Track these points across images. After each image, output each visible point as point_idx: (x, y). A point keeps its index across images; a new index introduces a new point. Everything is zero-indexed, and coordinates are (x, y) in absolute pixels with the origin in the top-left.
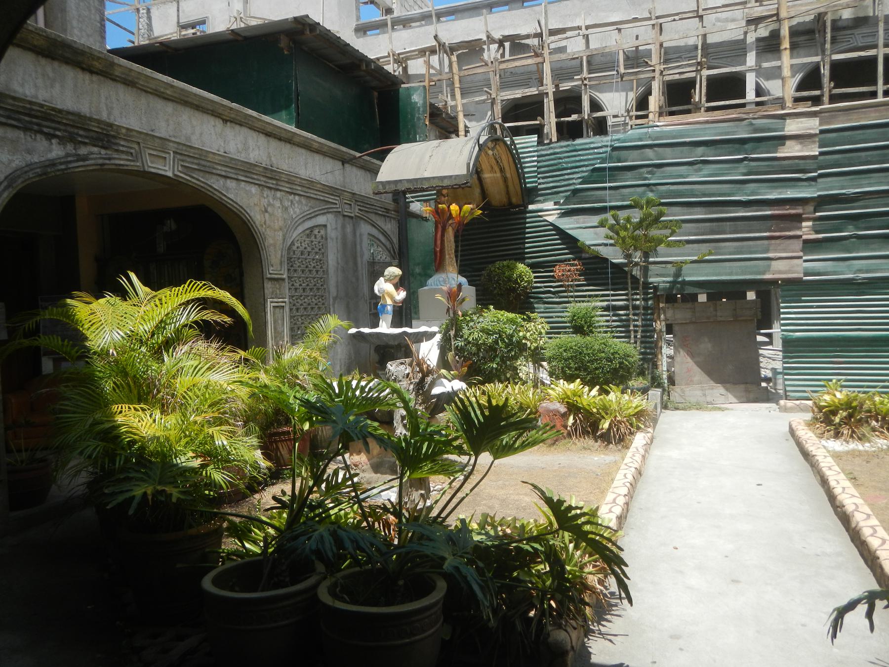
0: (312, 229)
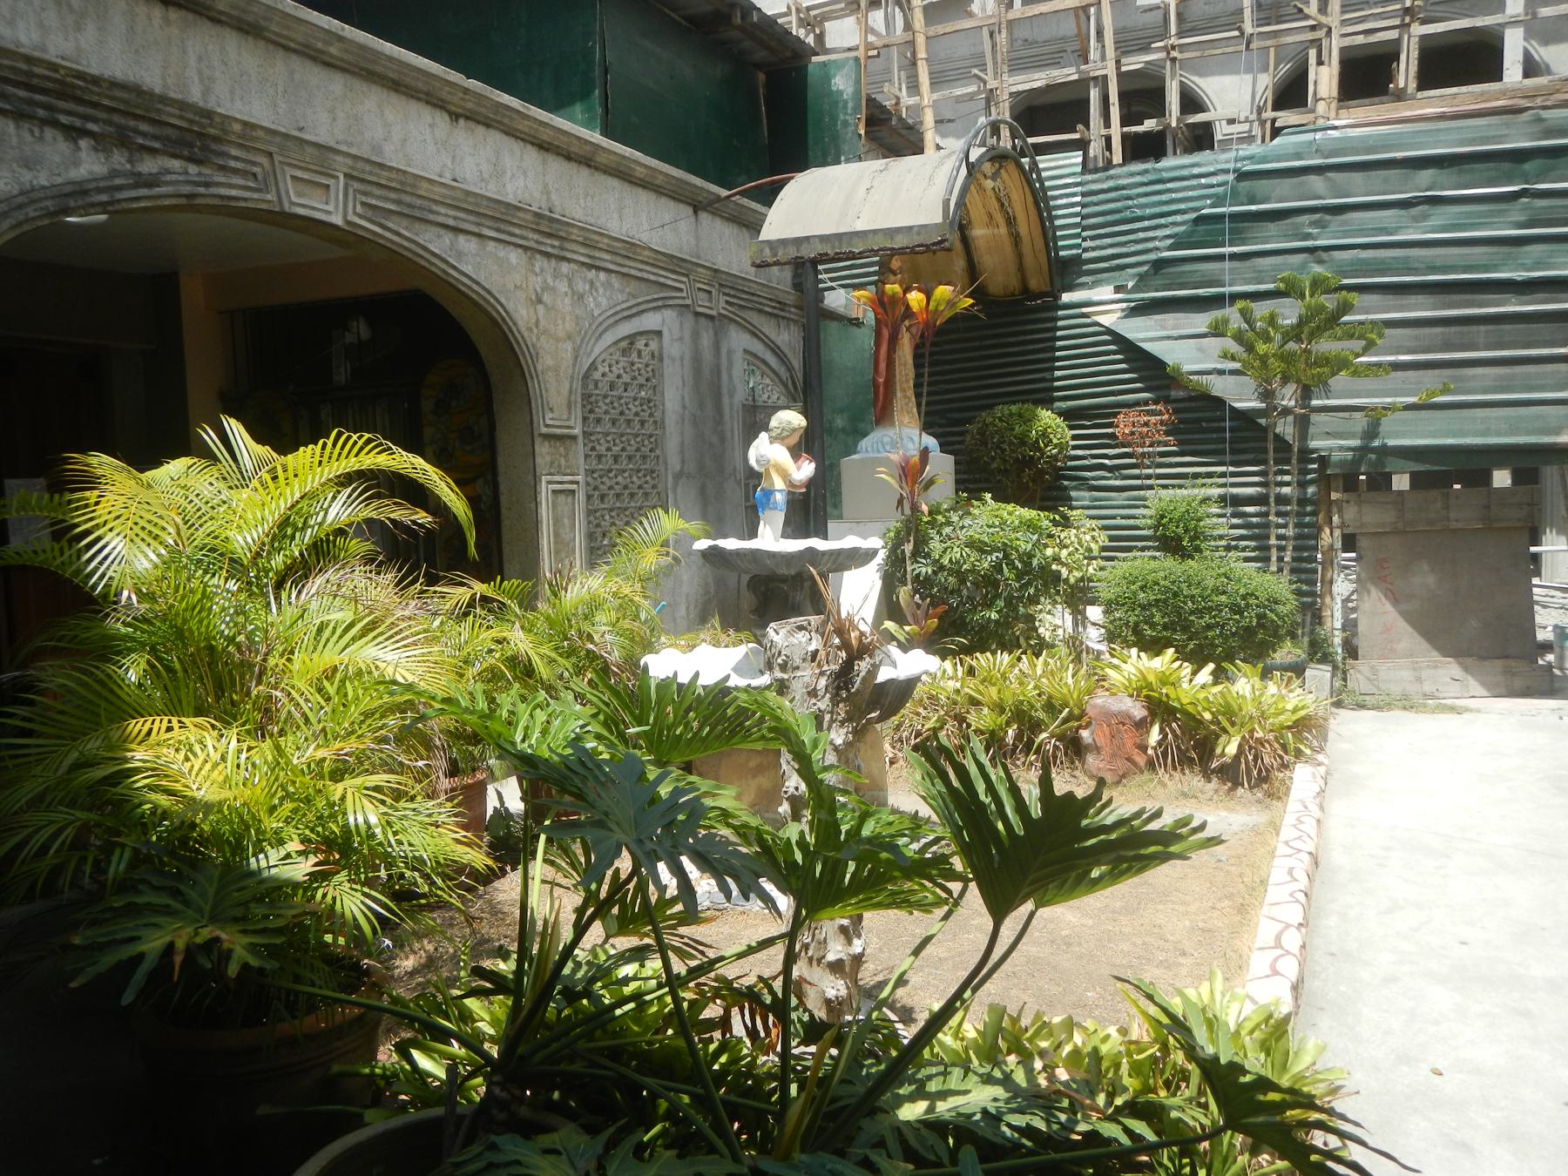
0: (632, 338)
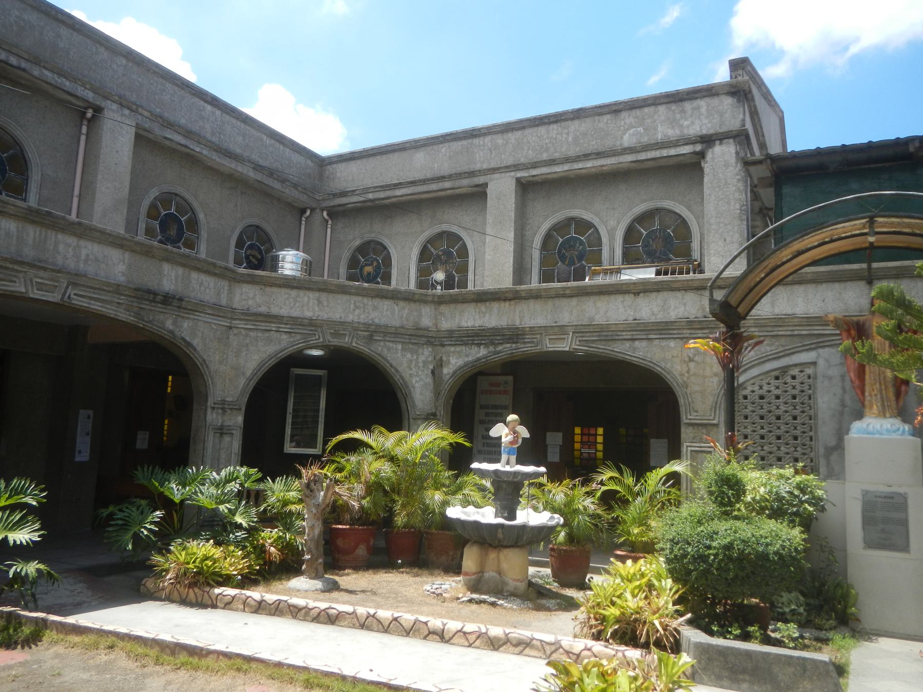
0: (784, 370)
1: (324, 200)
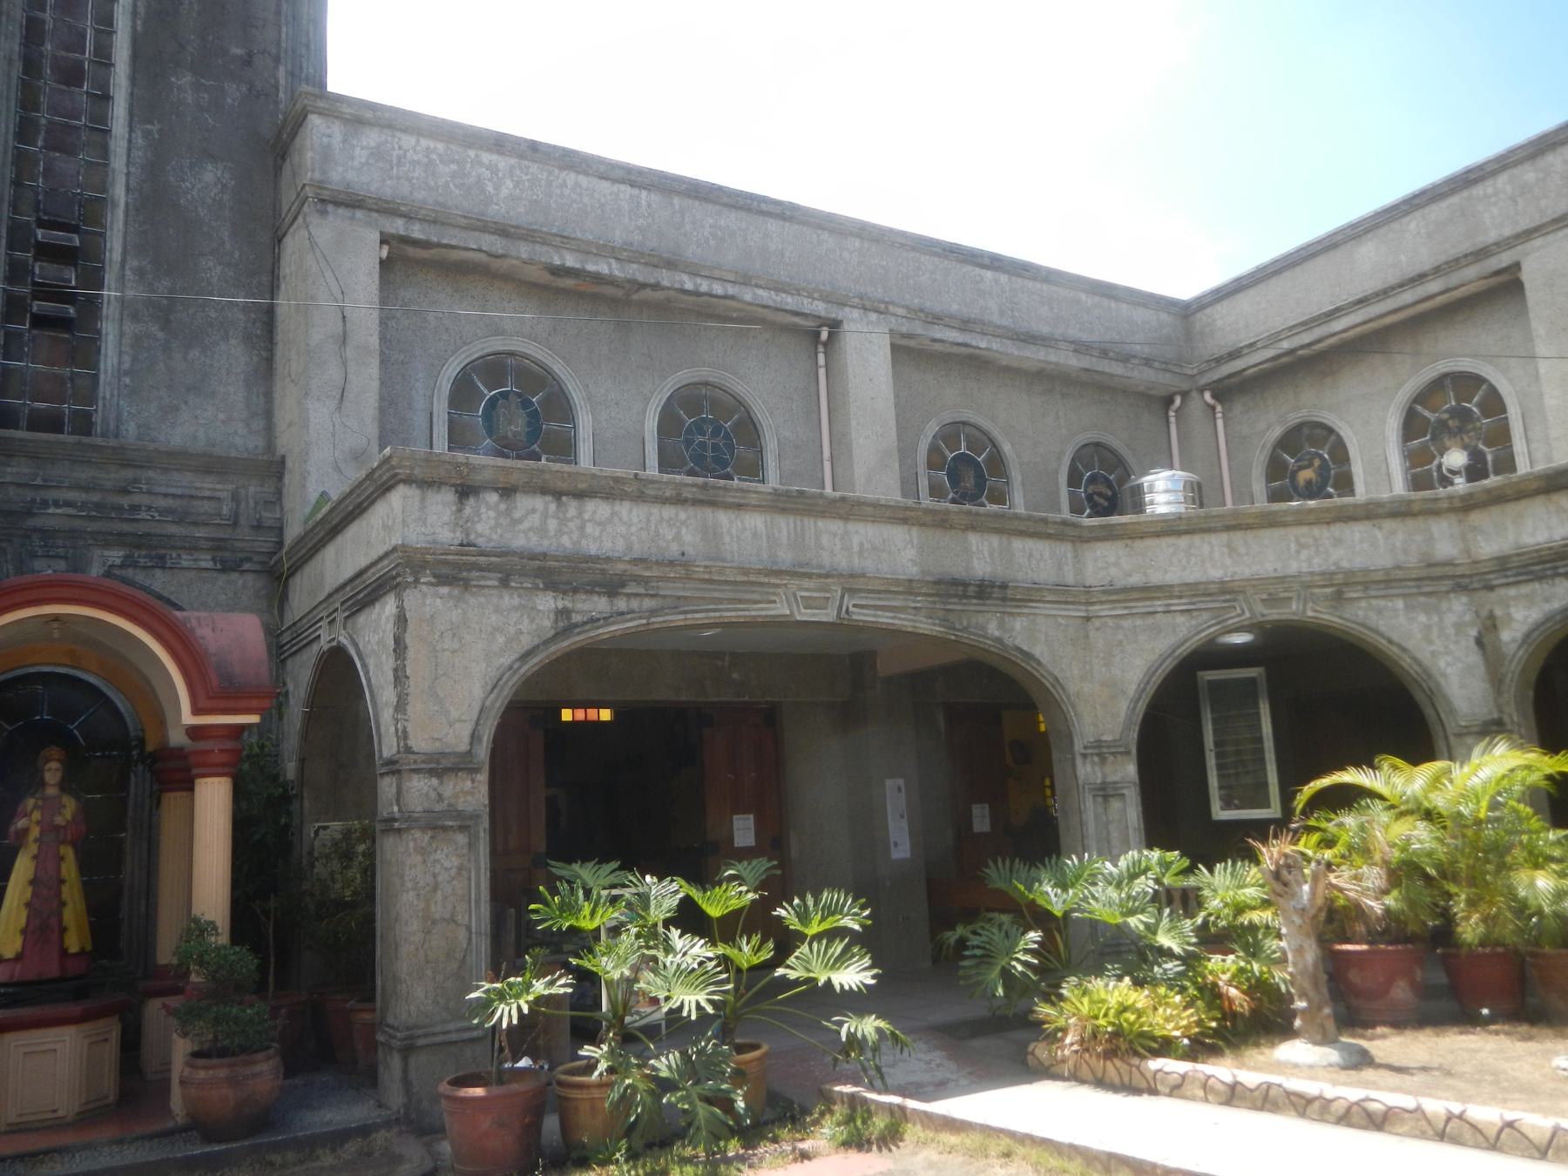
1: (1201, 373)
